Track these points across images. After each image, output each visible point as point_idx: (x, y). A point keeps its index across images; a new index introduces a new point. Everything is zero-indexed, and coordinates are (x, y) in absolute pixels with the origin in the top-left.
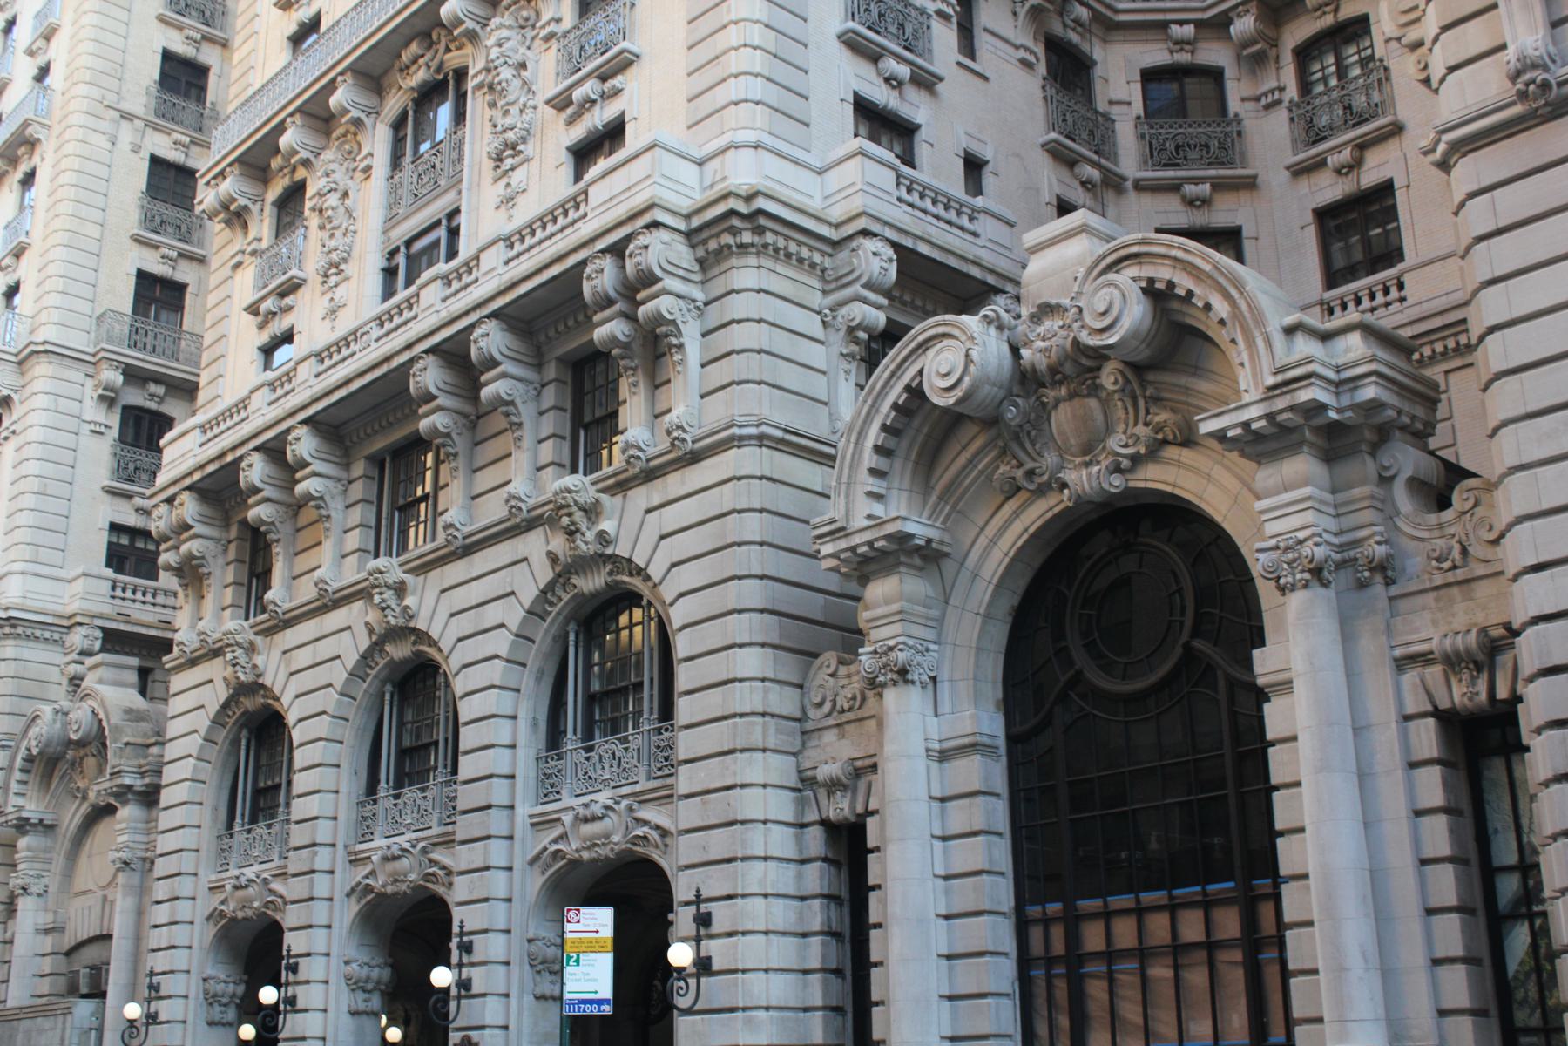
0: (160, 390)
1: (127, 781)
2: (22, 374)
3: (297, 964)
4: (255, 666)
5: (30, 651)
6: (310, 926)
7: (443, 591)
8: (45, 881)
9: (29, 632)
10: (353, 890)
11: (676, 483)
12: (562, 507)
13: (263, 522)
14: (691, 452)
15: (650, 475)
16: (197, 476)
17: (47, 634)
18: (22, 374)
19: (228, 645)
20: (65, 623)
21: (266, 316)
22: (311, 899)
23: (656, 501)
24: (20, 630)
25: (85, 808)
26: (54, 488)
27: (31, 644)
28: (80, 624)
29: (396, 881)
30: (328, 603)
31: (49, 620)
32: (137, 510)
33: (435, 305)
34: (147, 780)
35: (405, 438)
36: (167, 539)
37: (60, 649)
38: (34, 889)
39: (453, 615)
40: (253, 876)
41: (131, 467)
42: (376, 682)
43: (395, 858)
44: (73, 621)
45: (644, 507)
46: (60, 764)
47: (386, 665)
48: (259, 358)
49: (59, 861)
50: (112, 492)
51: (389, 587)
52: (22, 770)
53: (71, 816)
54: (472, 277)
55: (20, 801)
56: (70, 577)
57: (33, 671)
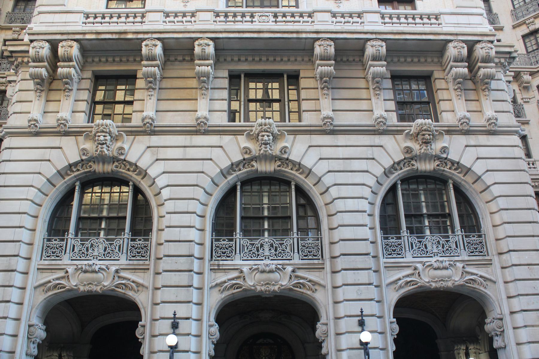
3: (178, 323)
4: (122, 148)
6: (189, 302)
7: (310, 146)
10: (217, 285)
11: (483, 139)
12: (428, 131)
14: (494, 131)
15: (467, 133)
16: (88, 37)
19: (103, 132)
22: (190, 286)
23: (473, 143)
29: (268, 284)
30: (201, 129)
35: (264, 70)
39: (321, 159)
40: (104, 267)
42: (236, 179)
43: (271, 271)
45: (466, 144)
47: (247, 172)
51: (272, 134)
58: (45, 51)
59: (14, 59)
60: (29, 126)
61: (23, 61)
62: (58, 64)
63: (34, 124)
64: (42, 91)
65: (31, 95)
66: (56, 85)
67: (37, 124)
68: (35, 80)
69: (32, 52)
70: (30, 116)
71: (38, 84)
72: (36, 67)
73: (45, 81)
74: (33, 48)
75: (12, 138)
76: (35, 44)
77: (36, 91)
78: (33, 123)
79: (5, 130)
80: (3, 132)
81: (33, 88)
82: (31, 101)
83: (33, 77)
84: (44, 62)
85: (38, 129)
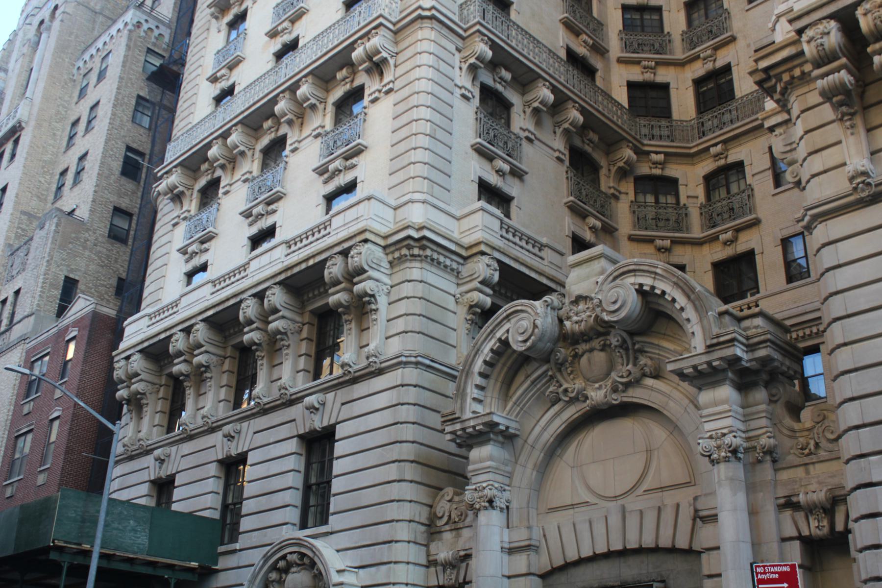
0: (508, 76)
1: (739, 351)
2: (396, 43)
5: (434, 277)
8: (506, 495)
9: (435, 256)
13: (182, 374)
17: (448, 262)
18: (396, 43)
20: (464, 253)
21: (191, 254)
24: (428, 252)
25: (572, 412)
26: (440, 134)
27: (434, 270)
28: (483, 253)
31: (453, 247)
32: (497, 172)
33: (342, 226)
34: (762, 353)
36: (122, 382)
37: (454, 279)
38: (499, 503)
41: (492, 134)
44: (475, 250)
46: (528, 369)
48: (184, 279)
49: (525, 474)
50: (480, 151)
52: (481, 374)
53: (549, 423)
54: (327, 231)
55: (479, 408)
56: (458, 214)
57: (436, 296)
58: (833, 36)
59: (774, 81)
60: (855, 189)
61: (792, 78)
62: (869, 50)
63: (863, 182)
64: (853, 115)
65: (835, 132)
66: (874, 93)
67: (869, 180)
68: (835, 99)
69: (809, 50)
70: (850, 169)
71: (841, 105)
72: (827, 74)
73: (853, 93)
74: (809, 42)
75: (829, 222)
76: (810, 33)
77: (841, 120)
78: (859, 180)
79: (809, 213)
80: (807, 219)
81: (834, 117)
82: (839, 142)
83: (828, 95)
84: (839, 58)
85: (874, 189)
